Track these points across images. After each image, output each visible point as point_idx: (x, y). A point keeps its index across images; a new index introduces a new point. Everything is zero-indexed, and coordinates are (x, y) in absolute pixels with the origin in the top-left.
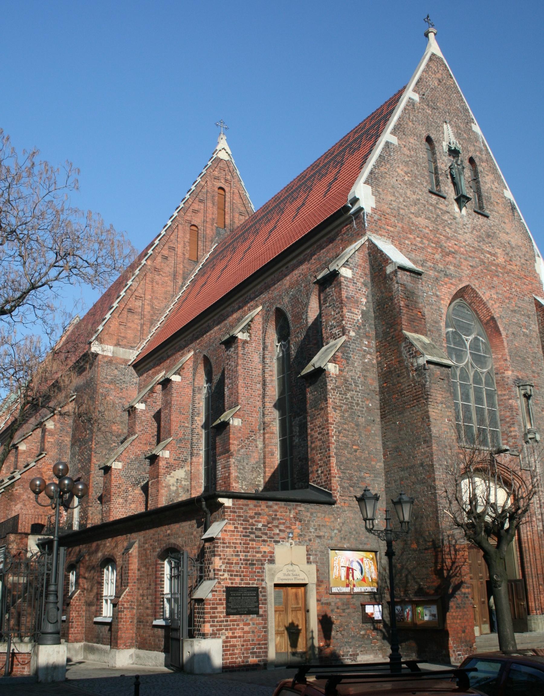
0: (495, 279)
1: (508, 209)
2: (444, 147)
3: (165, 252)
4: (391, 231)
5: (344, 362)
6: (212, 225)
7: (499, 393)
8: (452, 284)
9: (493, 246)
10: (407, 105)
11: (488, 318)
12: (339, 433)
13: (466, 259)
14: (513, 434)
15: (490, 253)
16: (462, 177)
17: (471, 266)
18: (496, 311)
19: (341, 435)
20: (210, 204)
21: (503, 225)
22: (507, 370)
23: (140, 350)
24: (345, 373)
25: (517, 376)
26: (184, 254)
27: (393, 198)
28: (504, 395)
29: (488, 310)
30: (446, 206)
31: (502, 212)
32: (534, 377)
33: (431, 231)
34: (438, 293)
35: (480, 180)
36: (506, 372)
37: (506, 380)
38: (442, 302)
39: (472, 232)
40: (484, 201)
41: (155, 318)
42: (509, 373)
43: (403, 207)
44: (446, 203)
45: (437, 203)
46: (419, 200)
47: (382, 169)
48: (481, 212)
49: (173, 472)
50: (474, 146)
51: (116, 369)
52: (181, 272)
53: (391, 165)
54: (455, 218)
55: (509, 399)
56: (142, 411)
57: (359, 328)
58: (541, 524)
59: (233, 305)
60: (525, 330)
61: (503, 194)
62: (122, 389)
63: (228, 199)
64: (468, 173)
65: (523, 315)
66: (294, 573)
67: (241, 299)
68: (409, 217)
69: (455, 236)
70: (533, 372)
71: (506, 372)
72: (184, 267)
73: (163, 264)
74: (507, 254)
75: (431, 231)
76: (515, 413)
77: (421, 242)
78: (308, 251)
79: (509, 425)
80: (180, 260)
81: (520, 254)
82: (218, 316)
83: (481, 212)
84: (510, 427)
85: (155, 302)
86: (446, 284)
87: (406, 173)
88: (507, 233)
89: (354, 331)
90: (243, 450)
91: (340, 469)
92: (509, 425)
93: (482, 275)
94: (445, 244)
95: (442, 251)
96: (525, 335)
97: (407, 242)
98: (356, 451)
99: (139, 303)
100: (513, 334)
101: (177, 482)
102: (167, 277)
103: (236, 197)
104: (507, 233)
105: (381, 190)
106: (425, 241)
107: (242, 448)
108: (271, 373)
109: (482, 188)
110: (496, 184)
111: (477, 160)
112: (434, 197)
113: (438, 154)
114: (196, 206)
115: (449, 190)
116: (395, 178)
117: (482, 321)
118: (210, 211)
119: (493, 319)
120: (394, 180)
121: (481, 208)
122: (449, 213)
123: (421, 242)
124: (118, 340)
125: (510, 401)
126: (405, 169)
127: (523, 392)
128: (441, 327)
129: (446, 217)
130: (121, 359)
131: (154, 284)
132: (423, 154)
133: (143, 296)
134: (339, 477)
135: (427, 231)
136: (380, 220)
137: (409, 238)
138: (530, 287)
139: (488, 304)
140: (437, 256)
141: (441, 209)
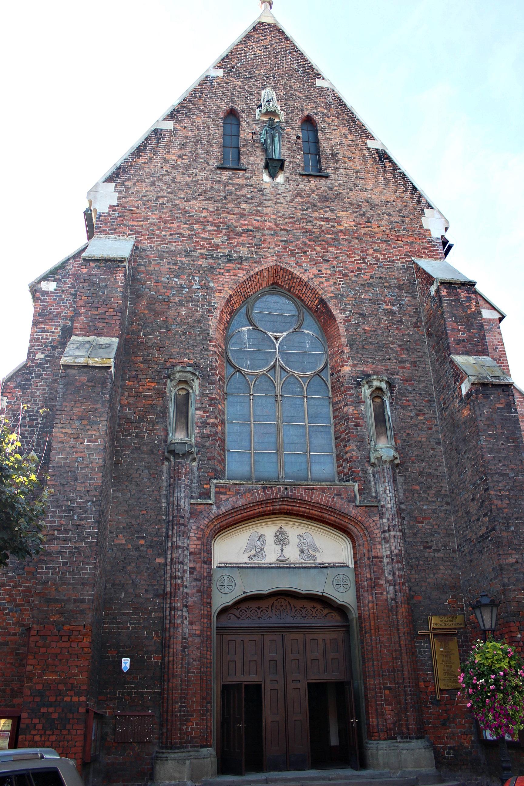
1: (370, 162)
9: (333, 211)
11: (317, 302)
14: (348, 455)
15: (327, 220)
17: (282, 241)
18: (327, 289)
21: (357, 182)
25: (363, 372)
27: (151, 188)
28: (340, 401)
31: (358, 167)
36: (341, 369)
37: (341, 379)
38: (217, 294)
39: (292, 201)
40: (324, 161)
42: (347, 369)
43: (165, 194)
44: (247, 175)
46: (197, 181)
47: (139, 161)
50: (316, 102)
53: (157, 153)
55: (345, 406)
58: (391, 588)
60: (389, 307)
76: (351, 425)
77: (191, 229)
79: (344, 443)
84: (345, 446)
86: (228, 271)
89: (43, 353)
92: (344, 443)
93: (306, 249)
97: (163, 233)
106: (196, 227)
109: (322, 145)
112: (225, 172)
116: (160, 166)
117: (311, 309)
119: (322, 301)
120: (158, 168)
122: (251, 186)
123: (191, 229)
125: (346, 409)
128: (209, 326)
132: (216, 130)
135: (204, 214)
139: (311, 284)
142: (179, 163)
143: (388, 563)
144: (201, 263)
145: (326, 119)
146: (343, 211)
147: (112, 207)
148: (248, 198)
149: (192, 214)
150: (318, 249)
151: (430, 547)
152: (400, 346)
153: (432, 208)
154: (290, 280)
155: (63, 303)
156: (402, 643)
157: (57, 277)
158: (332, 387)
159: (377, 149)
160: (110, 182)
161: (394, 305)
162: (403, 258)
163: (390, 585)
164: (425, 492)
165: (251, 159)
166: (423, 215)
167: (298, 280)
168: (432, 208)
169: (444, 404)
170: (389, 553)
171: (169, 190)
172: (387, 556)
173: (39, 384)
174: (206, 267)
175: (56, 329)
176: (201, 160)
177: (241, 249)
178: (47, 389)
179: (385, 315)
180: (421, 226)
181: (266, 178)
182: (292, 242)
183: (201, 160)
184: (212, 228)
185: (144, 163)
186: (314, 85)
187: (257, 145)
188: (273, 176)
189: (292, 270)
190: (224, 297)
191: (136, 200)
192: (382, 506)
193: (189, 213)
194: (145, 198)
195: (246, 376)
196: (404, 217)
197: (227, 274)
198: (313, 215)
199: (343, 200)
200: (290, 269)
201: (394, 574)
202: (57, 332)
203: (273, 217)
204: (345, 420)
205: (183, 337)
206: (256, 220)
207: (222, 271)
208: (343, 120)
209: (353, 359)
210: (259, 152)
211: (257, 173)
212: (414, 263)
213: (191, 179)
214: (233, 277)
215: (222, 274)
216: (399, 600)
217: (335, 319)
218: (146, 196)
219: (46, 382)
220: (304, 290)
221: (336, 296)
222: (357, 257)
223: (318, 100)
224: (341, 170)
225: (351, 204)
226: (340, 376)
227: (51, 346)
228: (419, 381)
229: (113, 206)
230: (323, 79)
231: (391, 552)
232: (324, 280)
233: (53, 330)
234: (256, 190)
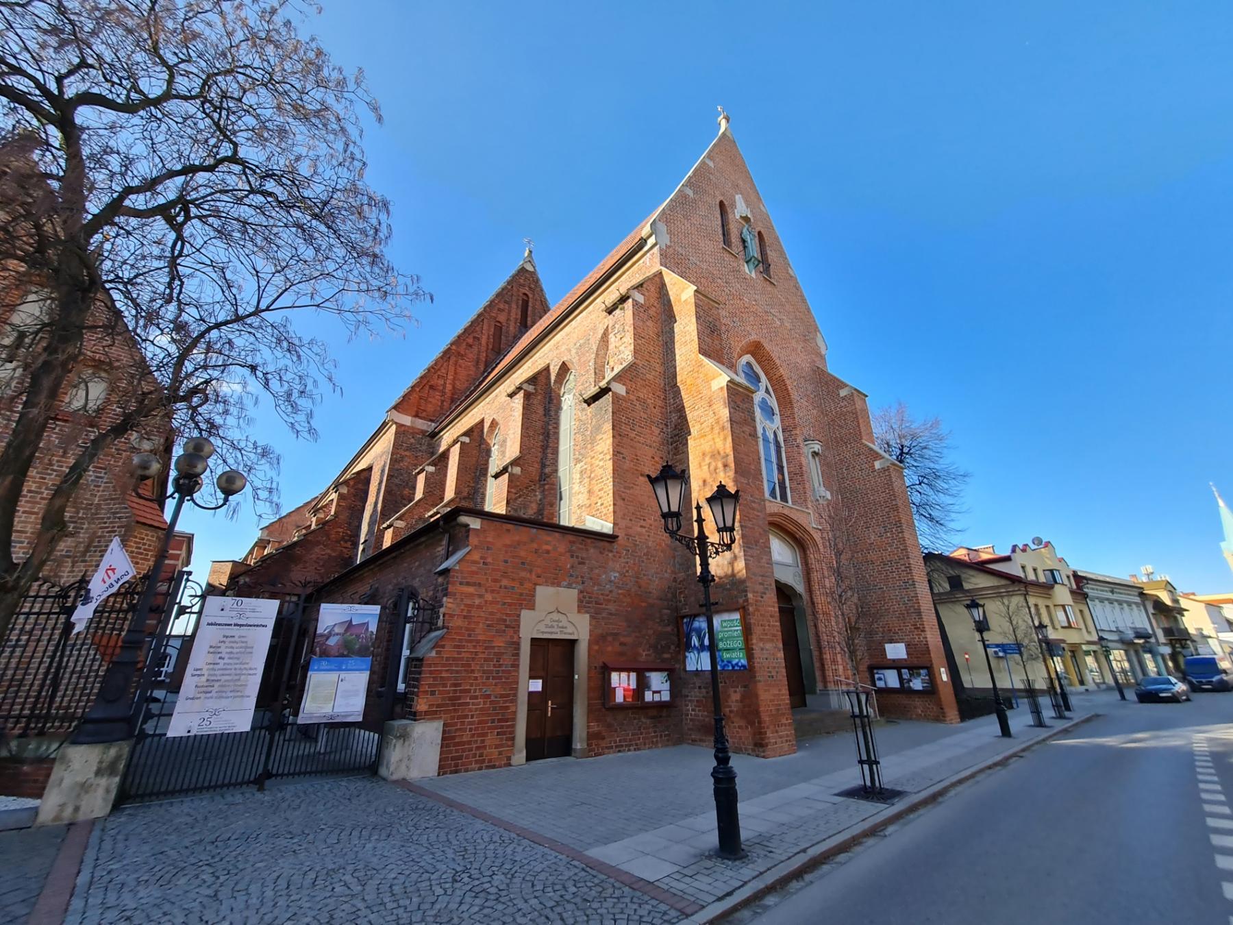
3: (470, 341)
20: (514, 306)
80: (483, 349)
85: (458, 383)
99: (441, 382)
103: (538, 303)
114: (502, 306)
118: (513, 311)
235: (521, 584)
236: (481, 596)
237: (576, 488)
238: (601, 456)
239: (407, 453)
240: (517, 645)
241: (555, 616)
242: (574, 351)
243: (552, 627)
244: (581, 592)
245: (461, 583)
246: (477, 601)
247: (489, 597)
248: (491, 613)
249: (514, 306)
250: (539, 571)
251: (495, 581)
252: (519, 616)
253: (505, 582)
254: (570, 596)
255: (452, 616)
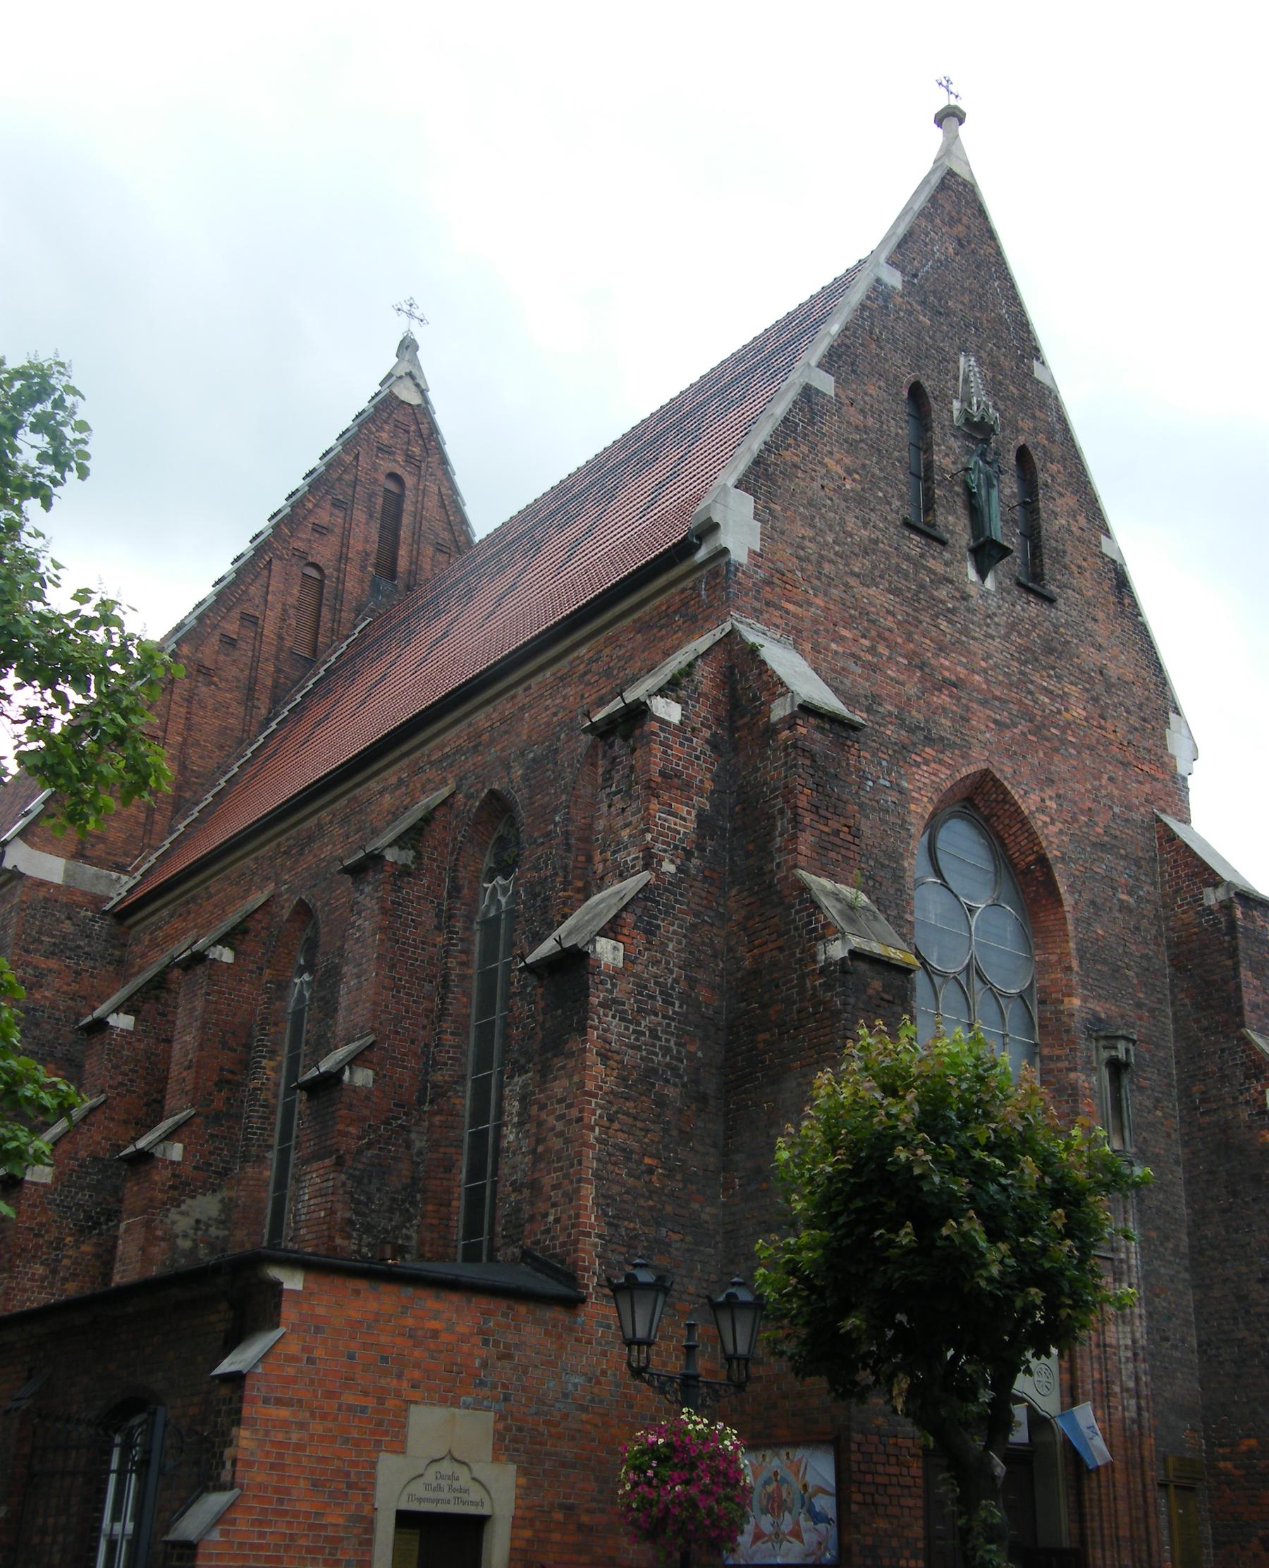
0: (1056, 759)
2: (956, 414)
3: (232, 628)
4: (795, 616)
5: (640, 939)
6: (363, 568)
7: (1046, 1052)
8: (941, 762)
9: (1059, 678)
10: (868, 298)
11: (1031, 858)
12: (611, 1120)
13: (984, 703)
15: (1048, 692)
16: (994, 493)
17: (995, 722)
18: (1053, 837)
19: (616, 1125)
20: (359, 515)
21: (1090, 624)
22: (1070, 995)
23: (138, 875)
24: (640, 968)
26: (281, 638)
28: (1059, 1058)
29: (1032, 837)
30: (947, 564)
31: (1090, 594)
32: (1140, 1018)
33: (899, 623)
34: (905, 784)
35: (1041, 505)
36: (1066, 1000)
37: (1066, 1019)
38: (913, 807)
39: (1006, 637)
41: (188, 795)
43: (832, 556)
44: (947, 555)
45: (922, 556)
46: (876, 542)
47: (787, 455)
48: (1033, 585)
49: (189, 1201)
50: (1034, 417)
51: (69, 918)
52: (269, 682)
53: (813, 446)
54: (966, 597)
56: (126, 1034)
57: (688, 854)
58: (1133, 1402)
59: (385, 774)
60: (1124, 897)
61: (1099, 545)
62: (78, 973)
63: (408, 506)
64: (1010, 486)
65: (1125, 858)
66: (456, 1484)
67: (405, 762)
68: (846, 584)
69: (962, 643)
70: (1139, 1005)
71: (1066, 1000)
72: (278, 671)
73: (221, 657)
74: (1096, 700)
75: (899, 623)
78: (583, 651)
80: (268, 649)
81: (1128, 703)
82: (344, 801)
83: (1036, 587)
86: (927, 763)
87: (849, 472)
88: (1100, 648)
89: (672, 862)
90: (370, 1153)
91: (606, 1214)
94: (933, 661)
95: (923, 680)
96: (1123, 907)
97: (834, 646)
98: (650, 1171)
100: (1093, 903)
101: (197, 1229)
102: (230, 690)
103: (431, 503)
104: (1100, 648)
105: (778, 508)
106: (882, 649)
107: (370, 1145)
108: (464, 958)
109: (1044, 525)
110: (1082, 520)
111: (1036, 455)
113: (937, 430)
114: (324, 517)
115: (954, 523)
118: (358, 532)
119: (1042, 861)
121: (1037, 576)
122: (951, 582)
123: (872, 650)
124: (81, 843)
125: (1072, 1075)
126: (848, 461)
127: (1105, 1055)
129: (942, 593)
130: (84, 894)
131: (195, 706)
132: (899, 428)
133: (161, 734)
134: (600, 1236)
135: (889, 622)
136: (768, 583)
137: (842, 638)
138: (1147, 788)
140: (911, 689)
141: (931, 571)
142: (848, 487)
143: (1127, 1359)
144: (888, 732)
145: (1049, 465)
146: (1072, 683)
147: (752, 553)
148: (949, 610)
149: (873, 617)
150: (1041, 754)
151: (1167, 1339)
152: (1137, 975)
153: (1178, 714)
154: (998, 802)
155: (697, 758)
156: (1149, 1494)
157: (683, 693)
158: (1040, 1026)
159: (1114, 562)
160: (746, 490)
161: (1131, 896)
162: (1143, 806)
163: (1131, 1397)
164: (1162, 1244)
165: (950, 518)
166: (1167, 723)
167: (1012, 809)
168: (1178, 714)
169: (1203, 1101)
170: (1129, 1342)
171: (837, 548)
172: (1126, 1347)
173: (671, 928)
174: (896, 744)
175: (689, 813)
176: (881, 494)
177: (943, 721)
178: (684, 941)
179: (1120, 911)
180: (1165, 748)
181: (973, 575)
182: (1008, 727)
183: (881, 494)
184: (901, 660)
185: (796, 466)
186: (1029, 374)
187: (957, 489)
188: (983, 575)
189: (1009, 787)
190: (922, 816)
191: (789, 551)
192: (1121, 1261)
193: (867, 614)
194: (802, 553)
195: (935, 977)
196: (1144, 720)
197: (925, 768)
198: (1034, 678)
199: (1071, 659)
200: (1006, 783)
201: (1137, 1380)
202: (691, 821)
203: (983, 664)
204: (1070, 1095)
205: (871, 883)
206: (960, 664)
207: (918, 759)
208: (1071, 475)
209: (1084, 987)
210: (961, 511)
211: (959, 557)
212: (1159, 820)
213: (867, 533)
214: (933, 778)
215: (918, 765)
216: (1145, 1423)
217: (1059, 902)
218: (803, 549)
219: (680, 927)
220: (1014, 829)
221: (1063, 859)
222: (1089, 786)
223: (1038, 413)
224: (1070, 592)
225: (1082, 672)
226: (1062, 1012)
227: (684, 849)
228: (1158, 1046)
229: (754, 552)
230: (1043, 363)
231: (1134, 1341)
232: (1048, 820)
233: (685, 814)
234: (958, 595)
235: (381, 1401)
236: (302, 1426)
237: (510, 1136)
238: (560, 1109)
239: (53, 964)
240: (368, 1524)
241: (446, 1467)
242: (518, 772)
243: (439, 1488)
244: (501, 1417)
245: (266, 1401)
246: (295, 1437)
247: (317, 1427)
248: (322, 1460)
249: (359, 515)
250: (417, 1374)
251: (330, 1395)
252: (373, 1465)
253: (349, 1398)
254: (471, 1428)
255: (250, 1464)
